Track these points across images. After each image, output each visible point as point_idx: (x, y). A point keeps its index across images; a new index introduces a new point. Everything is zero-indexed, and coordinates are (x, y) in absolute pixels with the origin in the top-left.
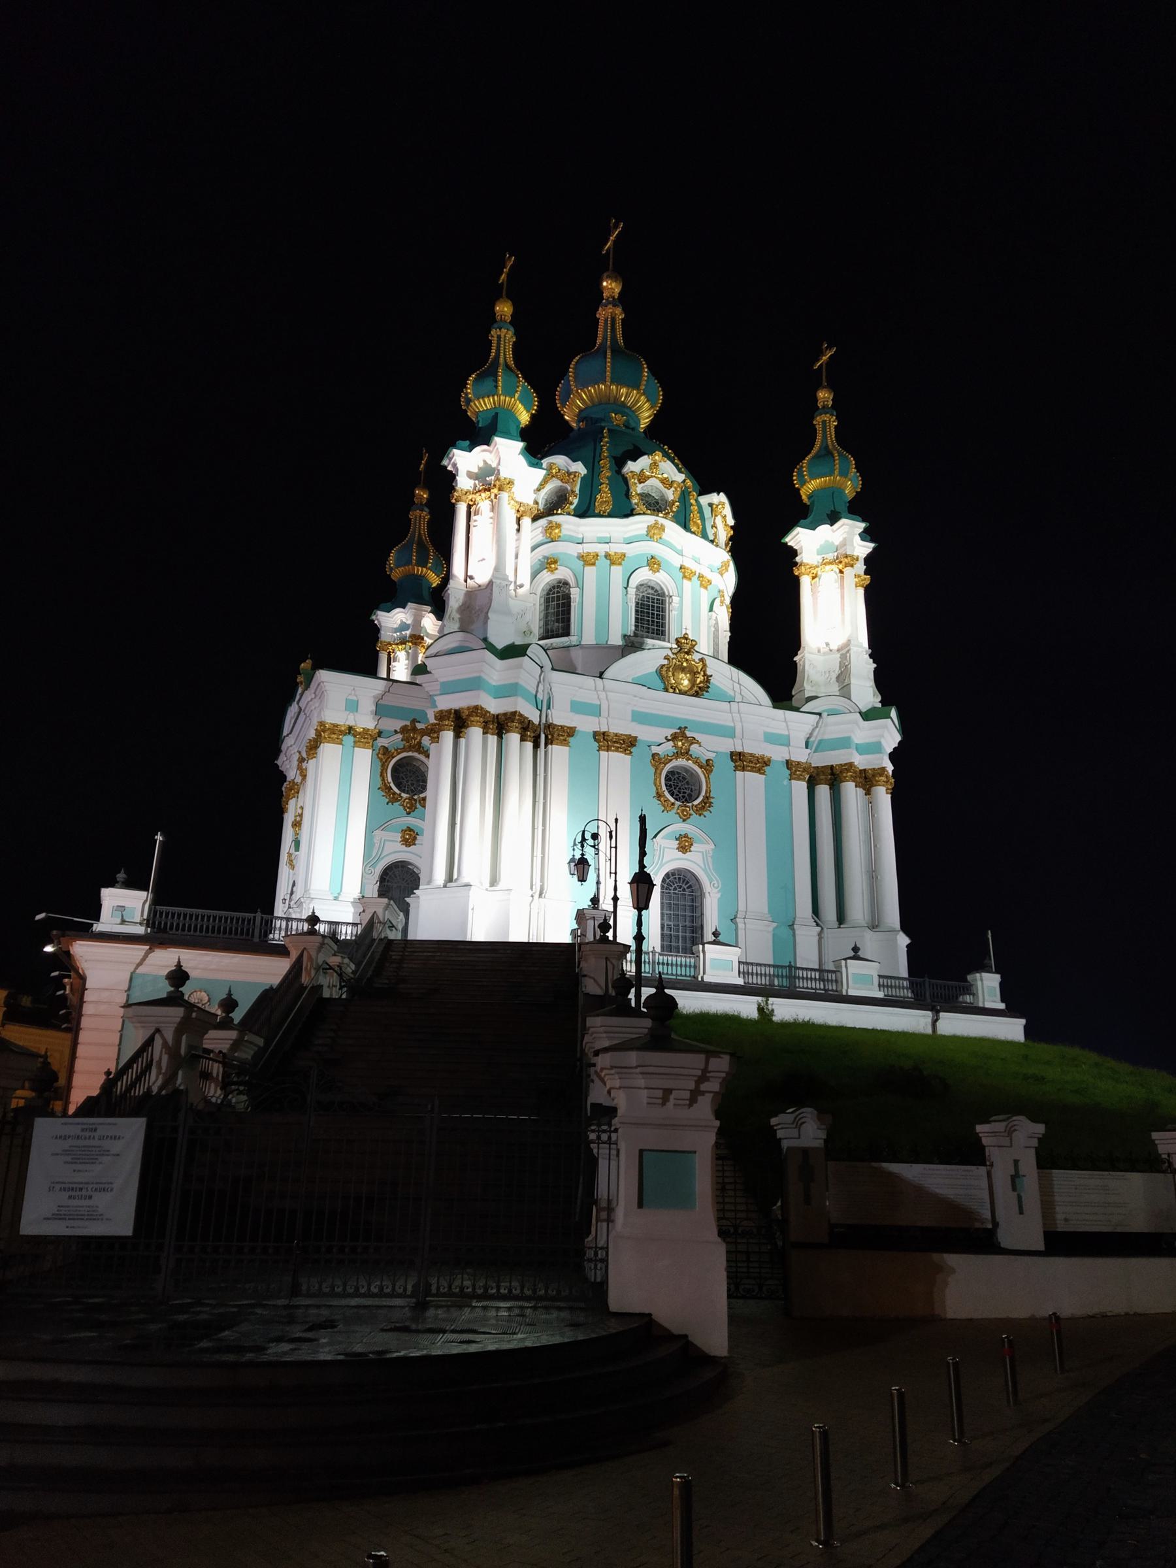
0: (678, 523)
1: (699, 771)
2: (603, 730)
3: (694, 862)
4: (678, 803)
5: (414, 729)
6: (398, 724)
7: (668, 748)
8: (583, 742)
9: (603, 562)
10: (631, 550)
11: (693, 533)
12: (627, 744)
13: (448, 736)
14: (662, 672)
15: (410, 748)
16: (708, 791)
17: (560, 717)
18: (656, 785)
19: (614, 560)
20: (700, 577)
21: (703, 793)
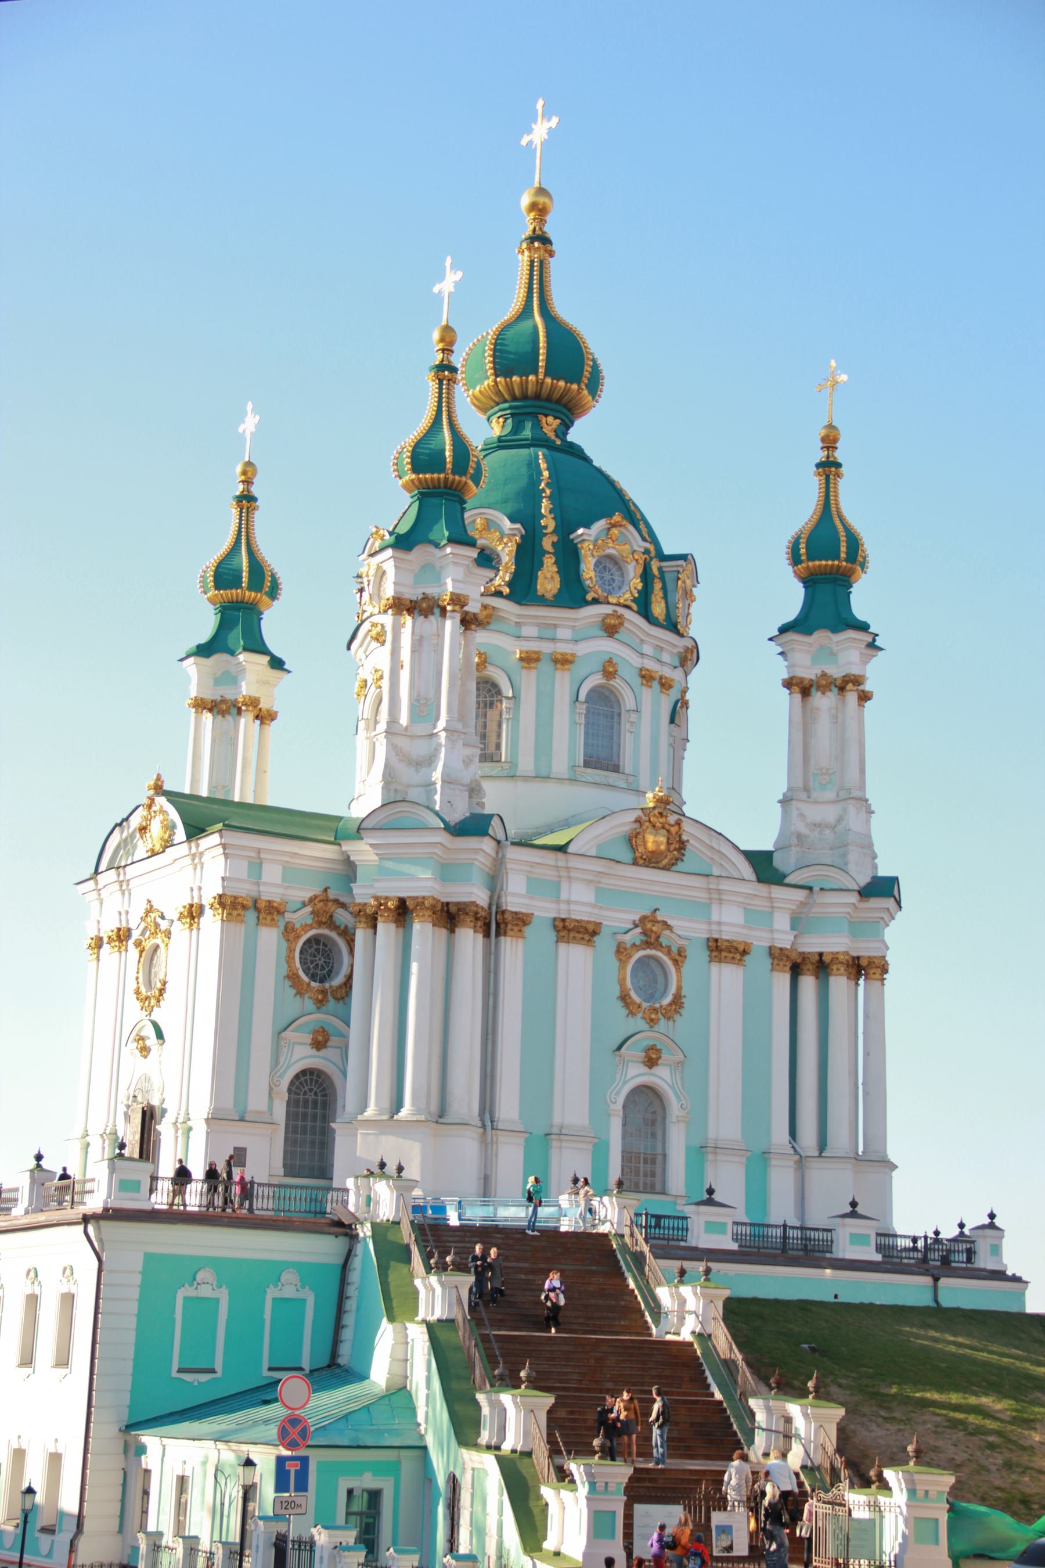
0: (638, 613)
1: (669, 963)
2: (563, 916)
3: (662, 1077)
4: (645, 1005)
5: (326, 900)
6: (307, 895)
7: (635, 936)
8: (540, 933)
9: (546, 666)
10: (581, 649)
13: (386, 930)
14: (633, 839)
15: (320, 924)
16: (679, 988)
17: (515, 900)
18: (622, 982)
19: (563, 661)
20: (661, 678)
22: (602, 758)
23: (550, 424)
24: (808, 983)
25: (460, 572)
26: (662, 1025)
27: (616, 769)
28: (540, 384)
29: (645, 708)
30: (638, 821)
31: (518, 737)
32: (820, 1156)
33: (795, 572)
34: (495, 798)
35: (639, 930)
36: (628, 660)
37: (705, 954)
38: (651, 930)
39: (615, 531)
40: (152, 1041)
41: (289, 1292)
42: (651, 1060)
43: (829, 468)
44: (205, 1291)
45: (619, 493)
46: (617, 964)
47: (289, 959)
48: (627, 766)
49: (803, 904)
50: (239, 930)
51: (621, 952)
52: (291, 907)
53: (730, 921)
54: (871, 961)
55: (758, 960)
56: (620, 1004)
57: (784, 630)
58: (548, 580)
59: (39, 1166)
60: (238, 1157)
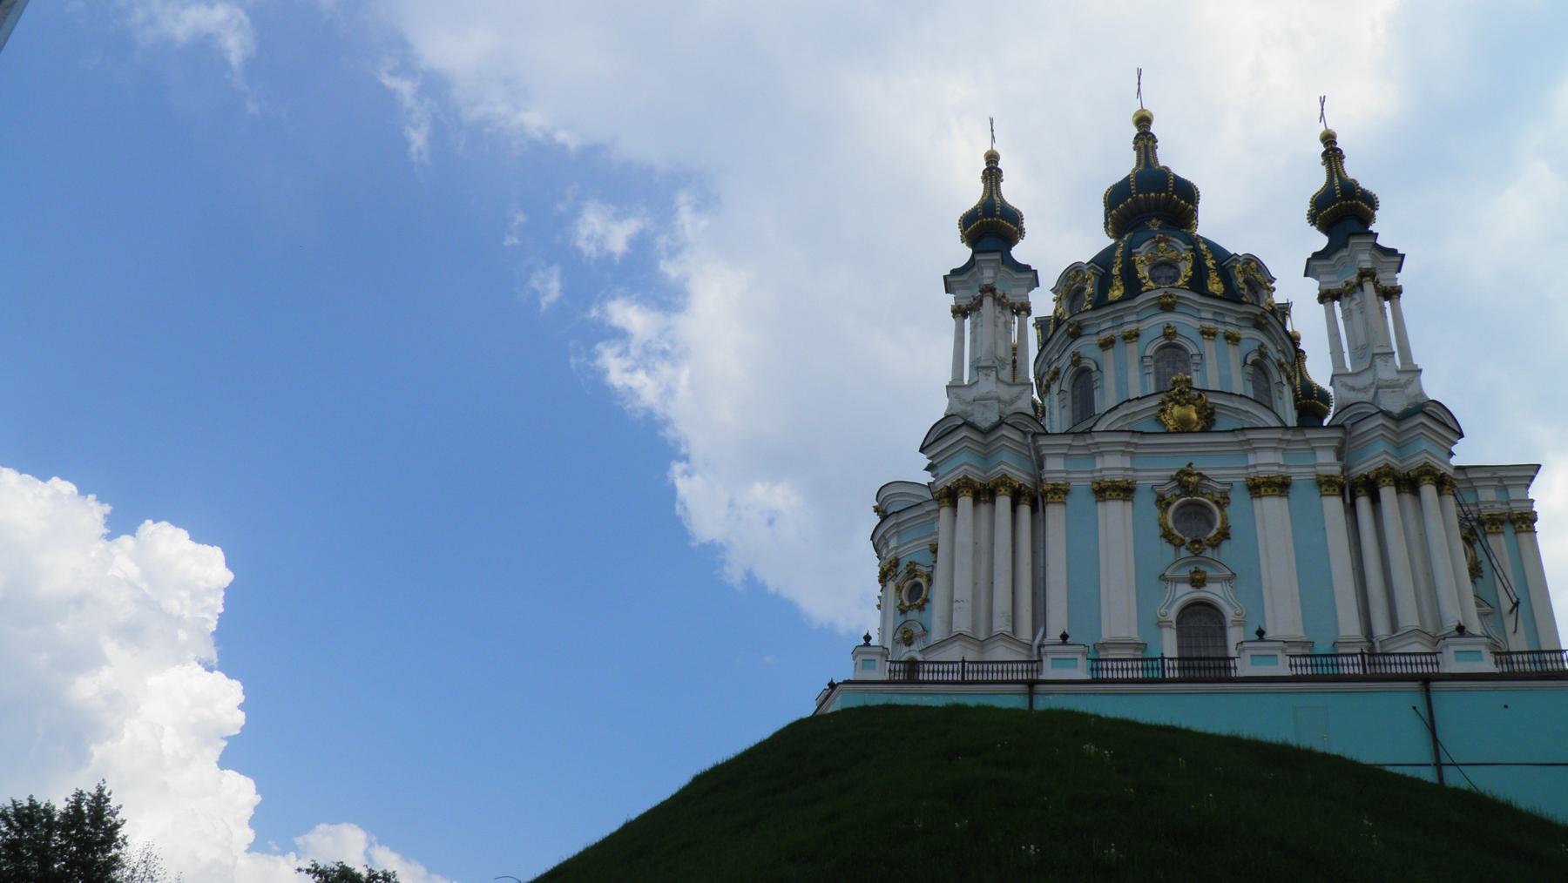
0: (1191, 290)
3: (1214, 592)
11: (1213, 296)
12: (1125, 491)
18: (1162, 525)
21: (1218, 524)
24: (1363, 503)
26: (1209, 553)
28: (1136, 201)
30: (1163, 403)
33: (1320, 229)
35: (1175, 484)
37: (1248, 496)
38: (1186, 482)
42: (1198, 581)
46: (1156, 512)
49: (1343, 442)
51: (1162, 502)
53: (1267, 462)
55: (1303, 489)
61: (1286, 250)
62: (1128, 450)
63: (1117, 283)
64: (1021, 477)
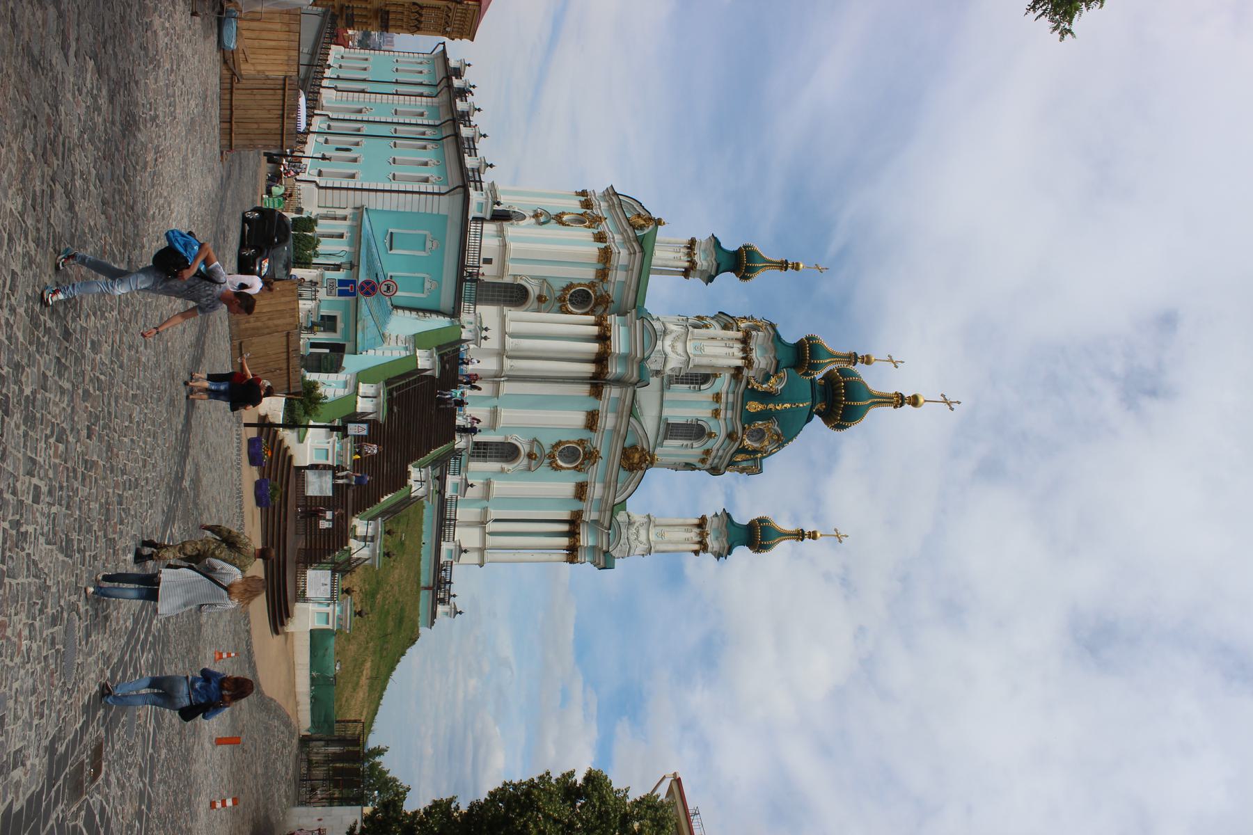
3: (523, 461)
4: (557, 454)
8: (592, 404)
11: (732, 456)
13: (595, 330)
22: (672, 430)
23: (821, 406)
24: (565, 528)
25: (763, 365)
26: (547, 461)
27: (665, 438)
28: (840, 402)
29: (694, 450)
30: (643, 449)
31: (681, 392)
32: (485, 533)
34: (655, 382)
36: (714, 444)
38: (591, 456)
39: (775, 437)
40: (542, 219)
41: (427, 285)
42: (530, 456)
43: (800, 535)
44: (429, 244)
45: (791, 439)
46: (575, 438)
47: (580, 285)
48: (667, 442)
49: (602, 525)
50: (595, 261)
52: (605, 286)
53: (596, 491)
54: (576, 557)
55: (577, 506)
56: (556, 440)
57: (728, 515)
58: (754, 406)
59: (487, 165)
60: (488, 261)
61: (748, 498)
62: (615, 430)
63: (760, 407)
64: (609, 377)
